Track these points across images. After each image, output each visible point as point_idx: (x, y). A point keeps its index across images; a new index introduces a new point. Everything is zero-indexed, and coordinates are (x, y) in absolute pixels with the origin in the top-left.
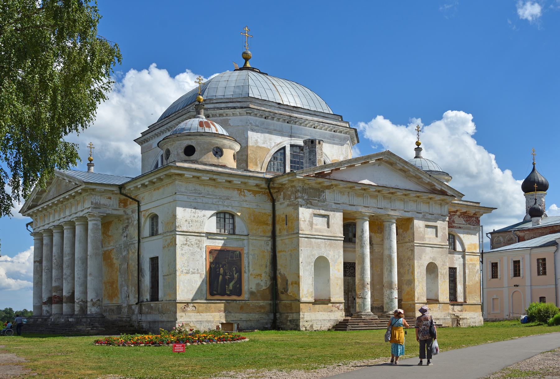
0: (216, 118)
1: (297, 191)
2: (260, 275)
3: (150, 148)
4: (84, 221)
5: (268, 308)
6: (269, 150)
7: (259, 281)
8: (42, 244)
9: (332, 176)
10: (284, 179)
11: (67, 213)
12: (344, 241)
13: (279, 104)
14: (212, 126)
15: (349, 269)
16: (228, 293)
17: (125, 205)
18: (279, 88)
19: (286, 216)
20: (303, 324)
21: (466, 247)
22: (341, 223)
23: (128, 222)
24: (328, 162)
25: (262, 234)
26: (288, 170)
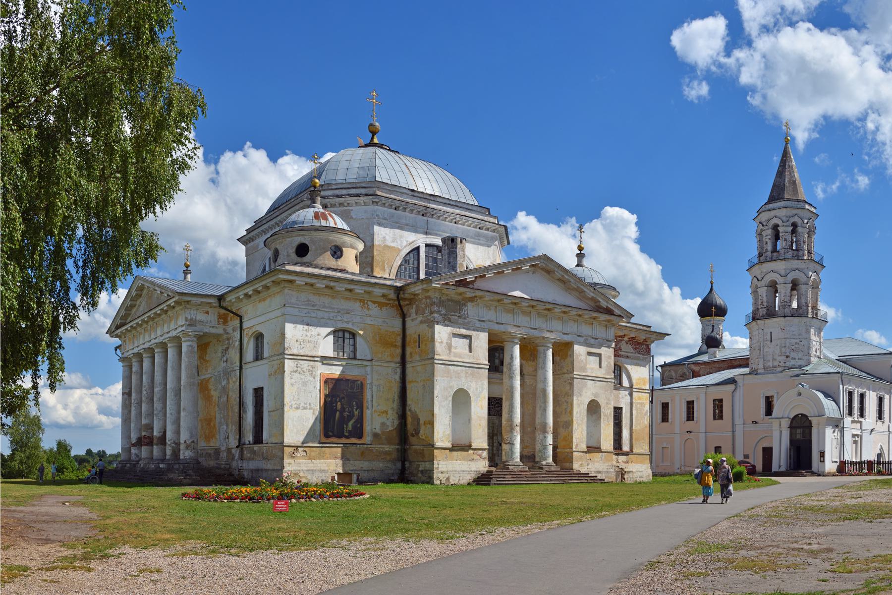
0: (335, 209)
1: (433, 304)
2: (386, 412)
3: (256, 249)
4: (177, 341)
5: (395, 455)
6: (400, 250)
7: (385, 420)
8: (131, 372)
9: (478, 284)
10: (417, 288)
11: (159, 333)
12: (489, 370)
13: (413, 191)
14: (330, 218)
15: (495, 405)
16: (347, 434)
17: (225, 322)
18: (412, 170)
20: (438, 476)
21: (634, 381)
22: (486, 346)
23: (229, 344)
24: (471, 267)
25: (389, 359)
26: (422, 276)
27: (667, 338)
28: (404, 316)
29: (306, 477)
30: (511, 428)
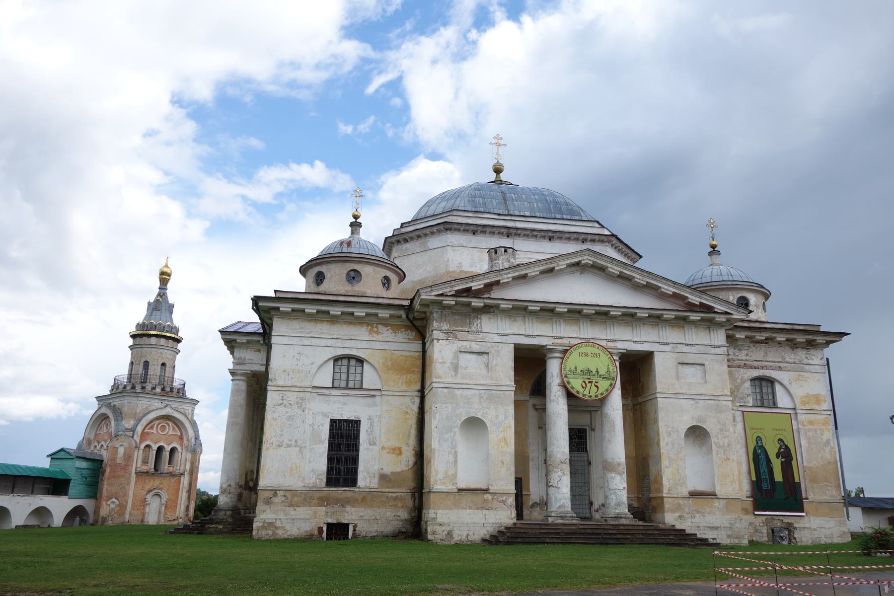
22: (511, 364)
25: (404, 387)
27: (845, 338)
29: (283, 528)
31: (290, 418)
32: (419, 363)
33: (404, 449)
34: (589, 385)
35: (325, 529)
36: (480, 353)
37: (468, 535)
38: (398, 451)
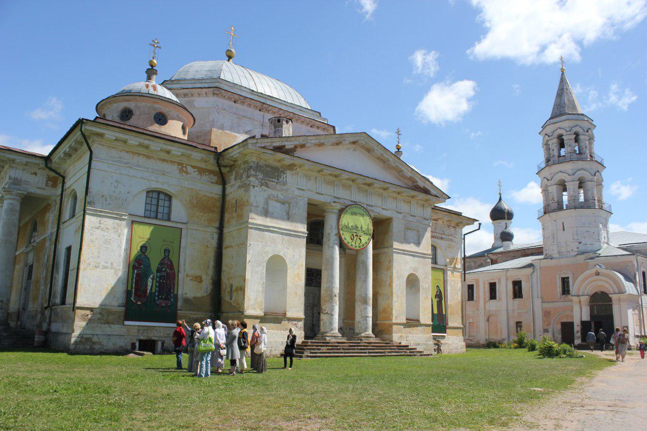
19: (237, 200)
28: (223, 182)
29: (100, 343)
30: (331, 297)
31: (107, 242)
32: (219, 204)
33: (204, 277)
34: (355, 238)
35: (137, 344)
36: (283, 203)
37: (271, 351)
38: (199, 279)
